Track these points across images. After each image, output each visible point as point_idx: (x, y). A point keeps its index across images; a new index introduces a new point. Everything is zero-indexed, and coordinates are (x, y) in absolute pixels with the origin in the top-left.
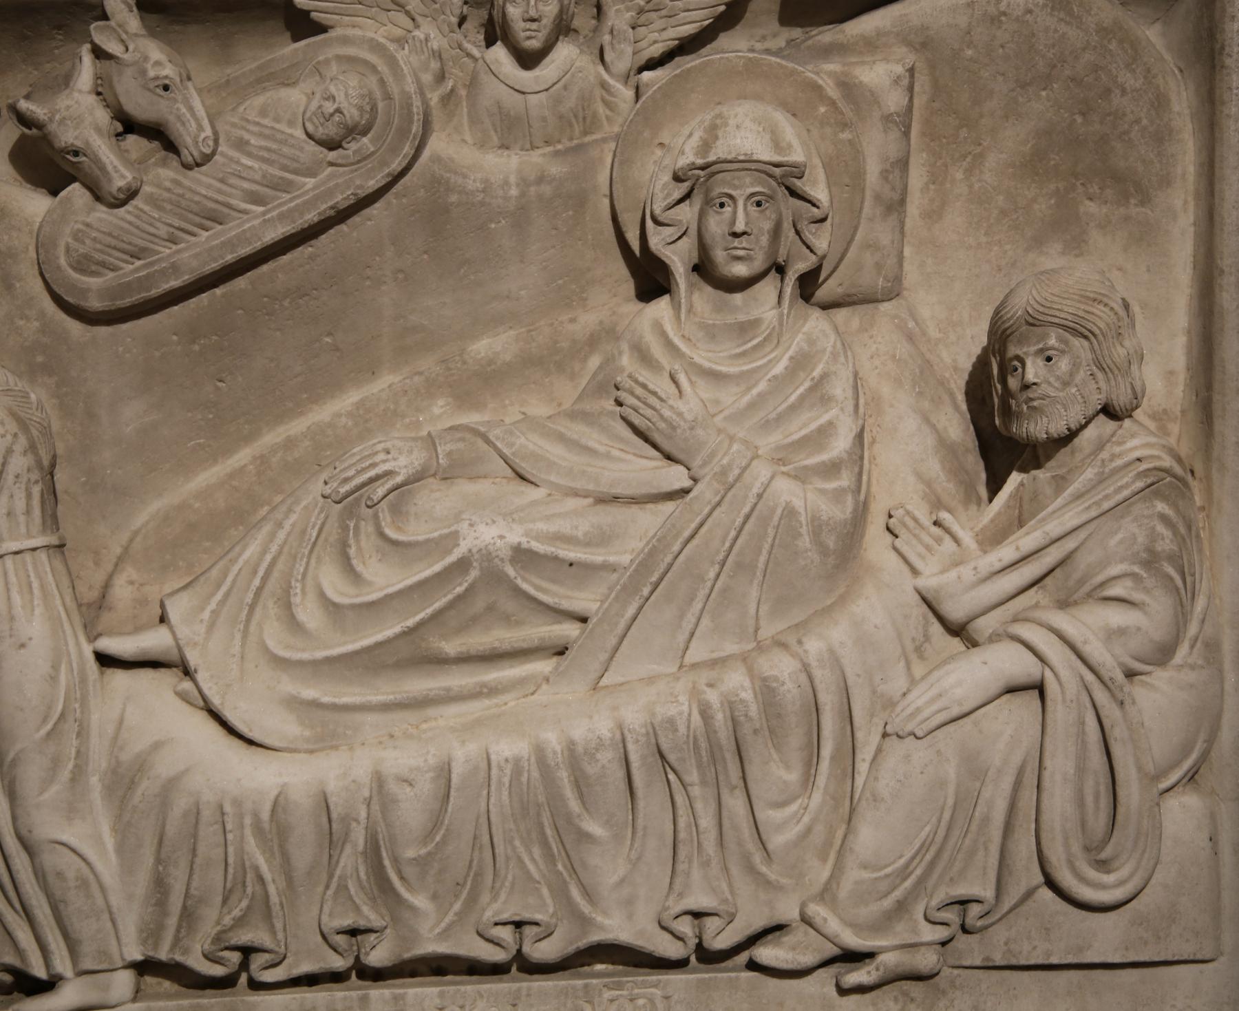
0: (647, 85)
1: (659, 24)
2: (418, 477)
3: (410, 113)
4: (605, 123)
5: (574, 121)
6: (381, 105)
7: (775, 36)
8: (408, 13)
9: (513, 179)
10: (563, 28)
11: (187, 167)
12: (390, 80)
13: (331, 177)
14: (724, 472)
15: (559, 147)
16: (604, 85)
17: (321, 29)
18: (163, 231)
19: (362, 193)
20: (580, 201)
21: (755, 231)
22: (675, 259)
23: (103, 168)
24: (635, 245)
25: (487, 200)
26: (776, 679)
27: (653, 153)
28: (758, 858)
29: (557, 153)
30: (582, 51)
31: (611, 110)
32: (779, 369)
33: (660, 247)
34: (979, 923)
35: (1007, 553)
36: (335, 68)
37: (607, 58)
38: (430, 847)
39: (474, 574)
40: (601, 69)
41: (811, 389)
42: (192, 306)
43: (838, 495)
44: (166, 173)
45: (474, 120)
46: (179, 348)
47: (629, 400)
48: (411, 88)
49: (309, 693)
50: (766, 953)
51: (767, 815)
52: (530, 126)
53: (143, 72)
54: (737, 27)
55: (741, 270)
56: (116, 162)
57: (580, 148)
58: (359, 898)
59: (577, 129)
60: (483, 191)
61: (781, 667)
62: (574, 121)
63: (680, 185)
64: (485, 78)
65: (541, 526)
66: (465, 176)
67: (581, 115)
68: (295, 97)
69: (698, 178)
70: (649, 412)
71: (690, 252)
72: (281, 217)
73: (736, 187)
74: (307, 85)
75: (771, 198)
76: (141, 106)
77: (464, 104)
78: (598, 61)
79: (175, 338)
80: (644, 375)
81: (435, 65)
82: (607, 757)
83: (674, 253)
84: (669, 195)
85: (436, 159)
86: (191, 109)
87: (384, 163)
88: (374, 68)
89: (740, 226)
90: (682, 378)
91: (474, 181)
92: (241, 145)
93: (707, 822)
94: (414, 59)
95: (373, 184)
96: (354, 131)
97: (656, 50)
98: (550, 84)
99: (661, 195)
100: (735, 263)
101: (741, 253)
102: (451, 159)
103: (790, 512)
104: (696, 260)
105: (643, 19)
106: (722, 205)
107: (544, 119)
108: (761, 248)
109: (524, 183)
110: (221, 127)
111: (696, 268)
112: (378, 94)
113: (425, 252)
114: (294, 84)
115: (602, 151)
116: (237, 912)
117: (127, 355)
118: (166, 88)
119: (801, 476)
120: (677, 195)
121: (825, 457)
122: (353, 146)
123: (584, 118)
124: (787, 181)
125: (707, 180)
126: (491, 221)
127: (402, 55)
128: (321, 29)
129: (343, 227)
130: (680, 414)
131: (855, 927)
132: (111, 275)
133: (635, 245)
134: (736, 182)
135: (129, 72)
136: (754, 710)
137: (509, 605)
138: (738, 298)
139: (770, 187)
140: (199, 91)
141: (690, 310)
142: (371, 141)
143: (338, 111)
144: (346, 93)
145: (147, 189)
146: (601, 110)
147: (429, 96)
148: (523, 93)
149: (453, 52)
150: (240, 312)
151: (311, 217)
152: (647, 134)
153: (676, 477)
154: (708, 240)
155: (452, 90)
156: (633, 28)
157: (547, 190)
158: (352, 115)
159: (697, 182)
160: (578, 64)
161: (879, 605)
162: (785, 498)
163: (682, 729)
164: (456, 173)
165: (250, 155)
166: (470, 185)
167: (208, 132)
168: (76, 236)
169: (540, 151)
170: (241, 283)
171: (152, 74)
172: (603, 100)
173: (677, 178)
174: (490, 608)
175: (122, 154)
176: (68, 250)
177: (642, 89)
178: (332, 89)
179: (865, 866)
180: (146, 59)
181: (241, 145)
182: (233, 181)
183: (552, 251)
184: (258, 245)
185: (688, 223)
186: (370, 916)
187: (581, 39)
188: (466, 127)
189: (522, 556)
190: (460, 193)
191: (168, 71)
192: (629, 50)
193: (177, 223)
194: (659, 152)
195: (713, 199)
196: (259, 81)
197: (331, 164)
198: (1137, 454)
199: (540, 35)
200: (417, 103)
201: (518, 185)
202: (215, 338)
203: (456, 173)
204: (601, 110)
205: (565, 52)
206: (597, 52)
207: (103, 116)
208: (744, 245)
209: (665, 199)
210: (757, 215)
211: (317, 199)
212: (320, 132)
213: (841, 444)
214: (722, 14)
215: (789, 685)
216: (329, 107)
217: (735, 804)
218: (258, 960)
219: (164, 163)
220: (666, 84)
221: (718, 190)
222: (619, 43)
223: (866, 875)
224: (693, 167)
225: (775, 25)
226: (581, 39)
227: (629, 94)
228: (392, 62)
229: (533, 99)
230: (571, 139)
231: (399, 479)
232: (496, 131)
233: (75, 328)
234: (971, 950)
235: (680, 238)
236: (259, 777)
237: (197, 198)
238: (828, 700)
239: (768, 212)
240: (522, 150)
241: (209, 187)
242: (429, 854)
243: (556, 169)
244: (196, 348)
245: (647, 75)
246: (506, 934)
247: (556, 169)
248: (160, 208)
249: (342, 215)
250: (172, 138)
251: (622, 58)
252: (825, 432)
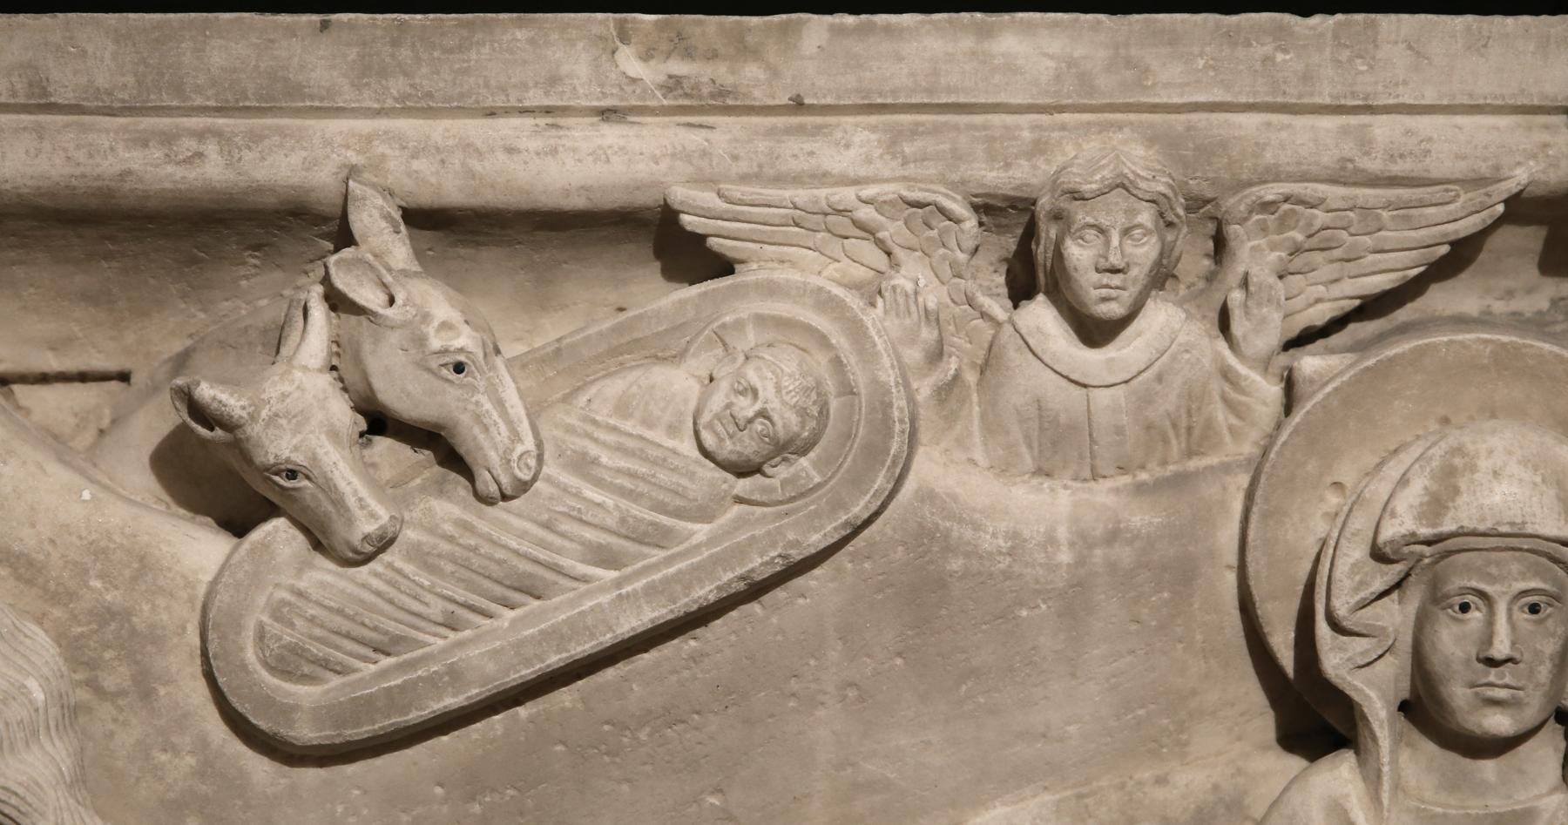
0: (1312, 381)
1: (1327, 271)
3: (887, 421)
4: (1227, 438)
5: (1171, 433)
6: (834, 404)
7: (1530, 291)
8: (880, 243)
9: (1062, 533)
10: (1161, 277)
11: (487, 501)
12: (851, 359)
13: (740, 523)
15: (1143, 476)
16: (1227, 374)
17: (724, 267)
18: (436, 608)
19: (797, 555)
20: (1183, 576)
21: (1527, 656)
22: (1372, 694)
23: (339, 502)
24: (1286, 658)
25: (1016, 569)
27: (1322, 499)
29: (1140, 489)
30: (1189, 317)
31: (1239, 416)
33: (1343, 672)
36: (751, 337)
37: (1238, 327)
40: (1222, 345)
42: (475, 736)
44: (448, 508)
45: (991, 427)
46: (445, 809)
48: (889, 376)
52: (1093, 441)
53: (420, 341)
54: (1464, 275)
55: (1499, 723)
56: (362, 484)
57: (1181, 481)
59: (1176, 447)
60: (1010, 553)
62: (1171, 433)
63: (1384, 567)
64: (1015, 356)
66: (977, 527)
67: (1183, 423)
68: (678, 383)
69: (1422, 556)
71: (1397, 680)
72: (651, 591)
73: (1493, 580)
74: (700, 363)
75: (1558, 598)
76: (406, 394)
77: (975, 397)
78: (1216, 331)
79: (439, 790)
81: (928, 334)
83: (1369, 683)
84: (1362, 584)
85: (927, 496)
86: (500, 403)
87: (838, 505)
88: (823, 341)
89: (1501, 648)
91: (994, 535)
92: (583, 465)
94: (892, 324)
95: (816, 540)
96: (786, 448)
97: (1320, 314)
98: (1134, 371)
99: (1347, 583)
100: (1489, 711)
101: (1502, 694)
102: (955, 498)
104: (1406, 695)
105: (1299, 262)
106: (1465, 608)
107: (1119, 430)
108: (1537, 685)
109: (1083, 541)
110: (546, 432)
111: (1405, 707)
112: (830, 385)
113: (899, 654)
114: (678, 357)
115: (1225, 489)
117: (351, 820)
118: (459, 368)
120: (1378, 585)
122: (782, 472)
123: (1189, 429)
125: (1436, 562)
126: (1022, 605)
127: (873, 318)
128: (724, 267)
129: (755, 607)
132: (336, 681)
133: (1286, 658)
134: (1494, 570)
135: (394, 338)
138: (1488, 768)
139: (1555, 581)
140: (509, 363)
141: (1397, 787)
142: (815, 465)
143: (763, 414)
144: (778, 385)
145: (410, 534)
146: (1221, 416)
147: (915, 385)
148: (1085, 386)
149: (957, 309)
150: (559, 748)
151: (705, 593)
152: (1312, 466)
154: (1436, 663)
155: (957, 377)
156: (1281, 277)
157: (1124, 554)
158: (787, 421)
159: (1424, 566)
160: (1182, 338)
164: (961, 521)
165: (598, 483)
166: (987, 543)
167: (529, 443)
168: (278, 612)
169: (1109, 483)
170: (565, 697)
171: (436, 343)
172: (1225, 400)
173: (1379, 555)
175: (367, 469)
176: (261, 635)
177: (1301, 388)
178: (752, 376)
180: (426, 317)
181: (583, 465)
182: (566, 526)
183: (1129, 658)
185: (1396, 631)
187: (1182, 290)
188: (977, 438)
190: (967, 555)
191: (465, 340)
192: (1276, 317)
193: (461, 594)
194: (1333, 500)
195: (1447, 597)
196: (614, 352)
197: (740, 500)
199: (1125, 294)
200: (899, 402)
201: (1072, 544)
202: (510, 792)
203: (961, 521)
204: (1221, 416)
205: (1161, 319)
206: (1214, 315)
207: (342, 414)
208: (1508, 680)
209: (1356, 590)
210: (1530, 627)
211: (717, 561)
212: (728, 449)
214: (1443, 258)
216: (745, 407)
219: (440, 490)
220: (1349, 383)
221: (1457, 582)
222: (1259, 305)
224: (1413, 539)
225: (1535, 272)
226: (1182, 290)
227: (1272, 391)
228: (857, 331)
229: (1102, 398)
230: (1164, 463)
232: (1030, 446)
233: (260, 768)
235: (1380, 657)
237: (500, 554)
239: (1550, 623)
240: (1075, 479)
241: (523, 535)
243: (1142, 517)
244: (476, 808)
245: (1310, 363)
247: (1142, 517)
248: (431, 569)
249: (756, 590)
250: (462, 451)
251: (1262, 329)
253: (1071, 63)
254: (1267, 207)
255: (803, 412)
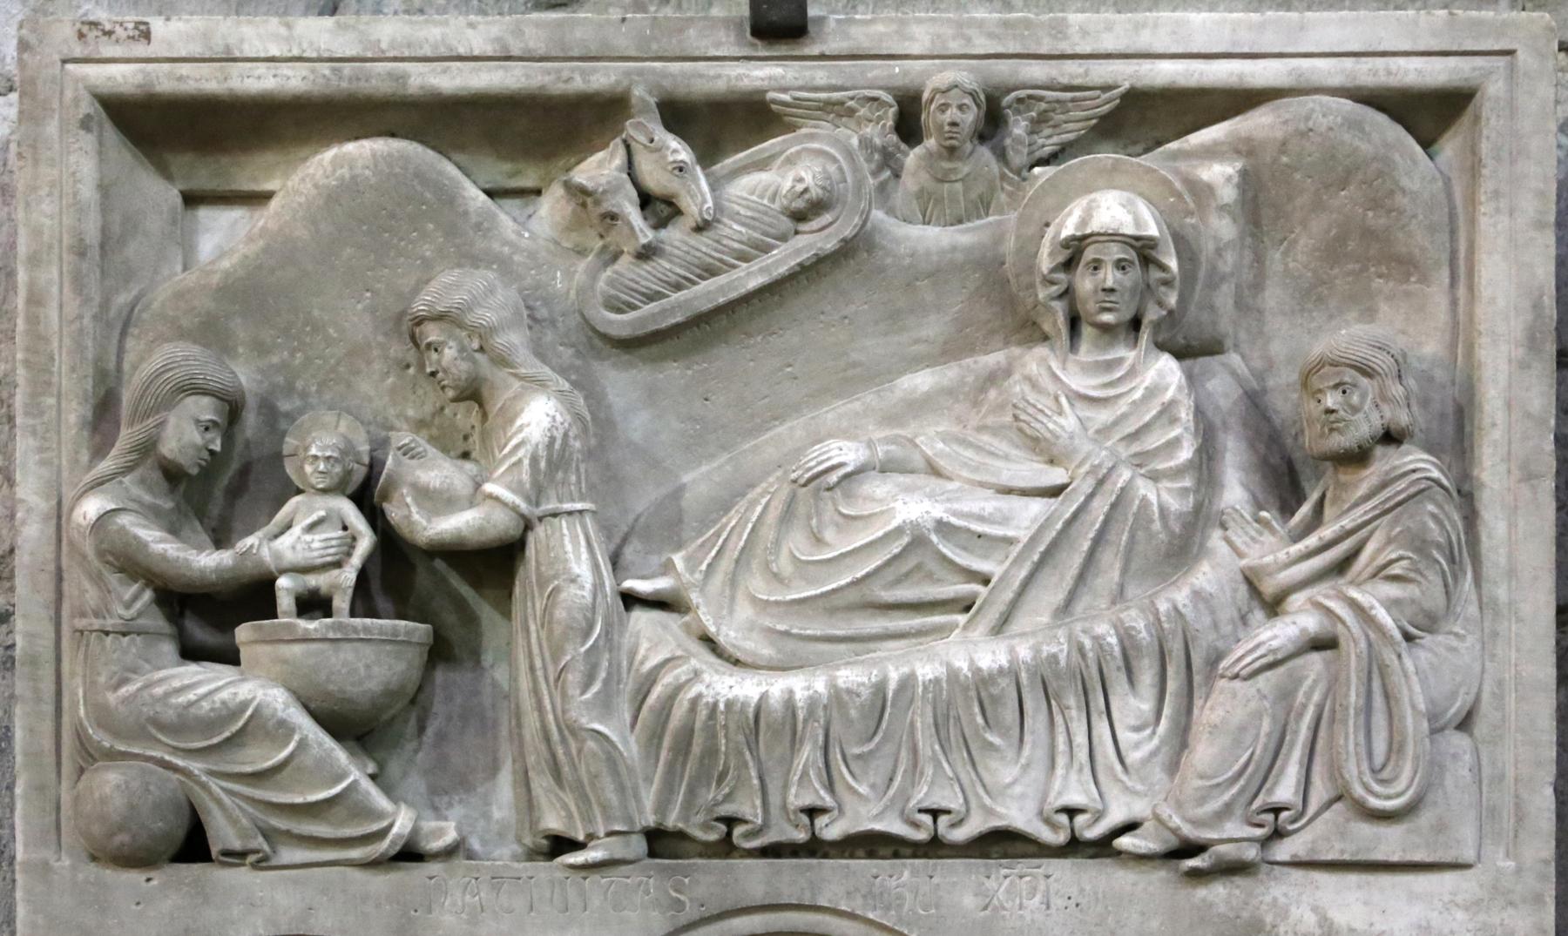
2: (860, 471)
14: (1094, 469)
26: (1133, 628)
28: (1118, 767)
32: (1137, 395)
34: (1291, 827)
35: (1312, 541)
38: (872, 745)
39: (906, 540)
41: (1161, 413)
43: (1184, 492)
47: (1023, 417)
49: (781, 627)
50: (1125, 842)
51: (1125, 736)
58: (817, 786)
61: (1137, 621)
65: (956, 506)
70: (1038, 426)
72: (761, 270)
80: (1032, 397)
82: (1005, 683)
88: (835, 160)
90: (1063, 400)
93: (1081, 739)
103: (1145, 502)
116: (727, 790)
118: (681, 170)
119: (1155, 477)
121: (1172, 464)
124: (1144, 251)
130: (1062, 427)
131: (1195, 823)
136: (1117, 650)
137: (932, 565)
153: (1057, 476)
161: (1212, 574)
162: (1142, 492)
163: (1063, 663)
171: (671, 159)
174: (919, 567)
179: (1201, 777)
184: (743, 291)
186: (828, 801)
189: (942, 527)
192: (1026, 151)
198: (1412, 467)
213: (1186, 453)
214: (1095, 126)
215: (1144, 634)
216: (800, 187)
217: (1102, 728)
218: (738, 831)
223: (1200, 783)
231: (849, 469)
234: (1284, 850)
236: (745, 688)
237: (698, 254)
238: (1176, 647)
242: (871, 752)
246: (927, 819)
252: (1174, 444)
253: (939, 36)
254: (1020, 100)
255: (824, 188)
